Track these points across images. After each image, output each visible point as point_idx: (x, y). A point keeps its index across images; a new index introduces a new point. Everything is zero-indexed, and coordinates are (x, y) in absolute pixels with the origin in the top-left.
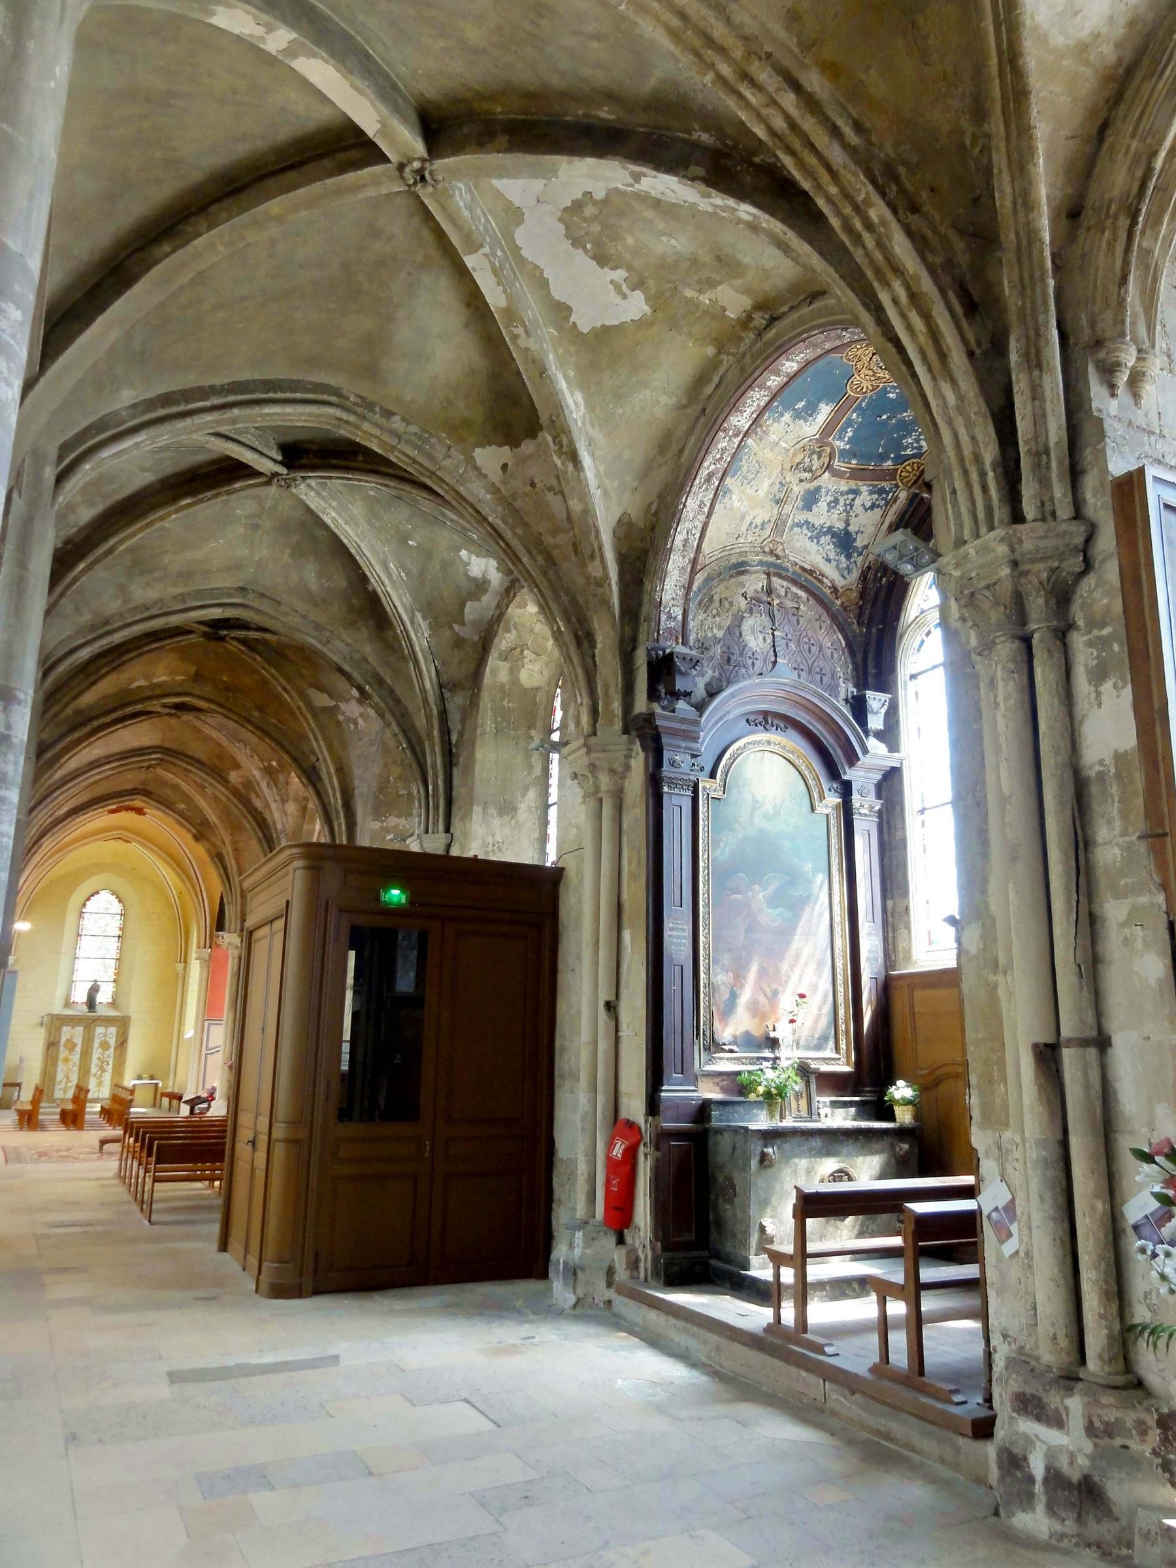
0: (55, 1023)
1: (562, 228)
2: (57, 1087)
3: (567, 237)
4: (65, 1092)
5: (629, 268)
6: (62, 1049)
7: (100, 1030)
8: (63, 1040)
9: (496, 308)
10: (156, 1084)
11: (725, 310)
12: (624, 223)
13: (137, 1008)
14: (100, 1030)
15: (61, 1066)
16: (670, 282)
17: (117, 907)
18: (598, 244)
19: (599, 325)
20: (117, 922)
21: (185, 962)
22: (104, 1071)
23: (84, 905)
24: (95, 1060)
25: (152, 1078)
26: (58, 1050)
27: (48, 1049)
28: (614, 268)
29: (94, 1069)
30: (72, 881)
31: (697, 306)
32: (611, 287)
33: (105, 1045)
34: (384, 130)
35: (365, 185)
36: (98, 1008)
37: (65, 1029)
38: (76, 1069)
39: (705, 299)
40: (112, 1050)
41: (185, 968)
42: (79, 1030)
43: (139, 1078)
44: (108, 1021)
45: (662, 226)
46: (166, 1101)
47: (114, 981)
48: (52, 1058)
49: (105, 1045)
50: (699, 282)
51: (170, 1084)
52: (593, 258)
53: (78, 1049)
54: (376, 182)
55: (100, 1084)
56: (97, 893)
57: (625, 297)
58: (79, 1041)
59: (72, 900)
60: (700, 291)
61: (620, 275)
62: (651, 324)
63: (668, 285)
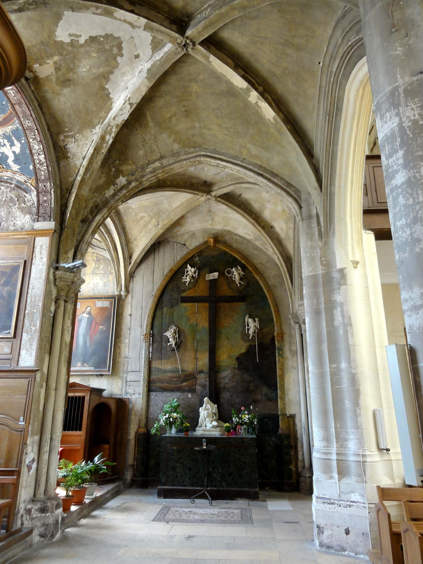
1: (116, 35)
3: (111, 35)
5: (82, 46)
9: (117, 11)
11: (40, 65)
12: (102, 58)
16: (66, 55)
18: (100, 43)
19: (64, 18)
28: (86, 41)
31: (48, 57)
32: (78, 34)
34: (207, 59)
35: (203, 30)
39: (51, 62)
45: (94, 71)
50: (60, 65)
52: (96, 37)
54: (199, 33)
57: (70, 35)
60: (55, 63)
61: (82, 41)
62: (49, 36)
63: (65, 53)
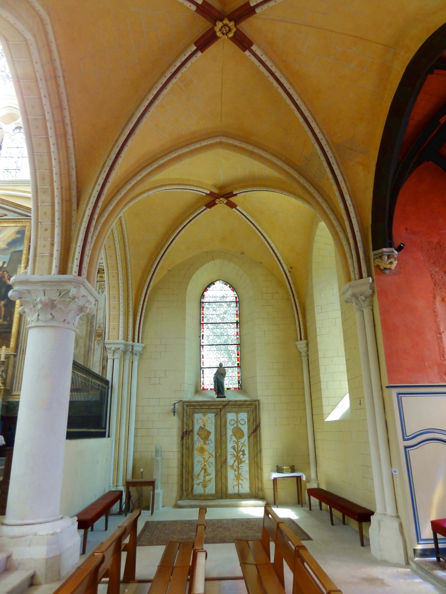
0: (187, 410)
2: (196, 481)
4: (205, 487)
6: (196, 437)
7: (231, 416)
10: (299, 478)
13: (266, 391)
14: (231, 416)
15: (197, 457)
17: (231, 295)
20: (233, 309)
21: (306, 338)
22: (241, 462)
23: (203, 296)
24: (230, 450)
25: (293, 470)
26: (193, 439)
27: (182, 438)
29: (230, 461)
30: (188, 269)
33: (238, 433)
36: (227, 393)
37: (197, 416)
38: (212, 460)
40: (246, 437)
41: (307, 344)
42: (211, 416)
43: (279, 470)
44: (238, 406)
46: (315, 501)
47: (239, 366)
48: (188, 449)
49: (238, 433)
51: (313, 475)
53: (212, 437)
55: (238, 477)
56: (213, 283)
58: (211, 428)
59: (189, 288)
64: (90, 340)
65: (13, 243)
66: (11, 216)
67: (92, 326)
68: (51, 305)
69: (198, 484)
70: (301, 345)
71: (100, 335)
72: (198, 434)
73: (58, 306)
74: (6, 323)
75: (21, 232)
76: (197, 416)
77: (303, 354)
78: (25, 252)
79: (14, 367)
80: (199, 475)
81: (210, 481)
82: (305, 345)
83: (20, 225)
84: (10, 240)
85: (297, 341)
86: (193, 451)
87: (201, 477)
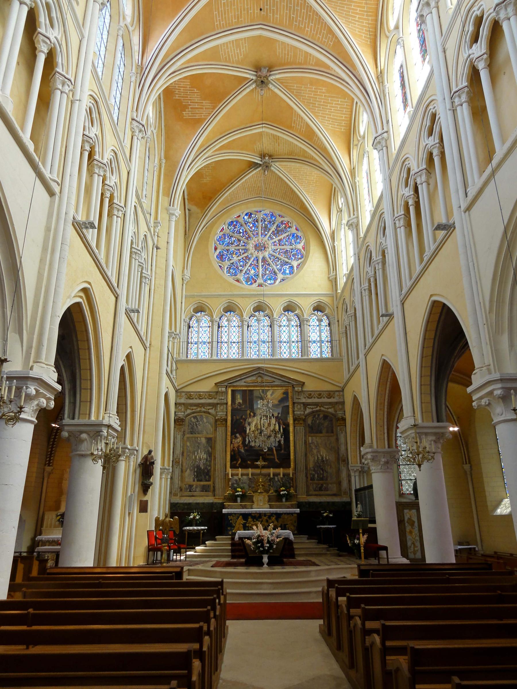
2: (409, 551)
4: (415, 554)
6: (406, 524)
8: (406, 519)
15: (409, 537)
21: (470, 463)
37: (406, 511)
41: (471, 467)
64: (339, 463)
65: (281, 401)
66: (277, 383)
67: (339, 455)
68: (387, 463)
69: (411, 553)
70: (467, 467)
71: (344, 461)
72: (407, 522)
73: (390, 462)
74: (286, 453)
75: (286, 393)
76: (406, 511)
77: (468, 473)
78: (291, 406)
79: (296, 481)
80: (410, 547)
81: (417, 551)
82: (469, 467)
83: (284, 388)
84: (280, 398)
85: (463, 464)
86: (405, 533)
87: (412, 549)
